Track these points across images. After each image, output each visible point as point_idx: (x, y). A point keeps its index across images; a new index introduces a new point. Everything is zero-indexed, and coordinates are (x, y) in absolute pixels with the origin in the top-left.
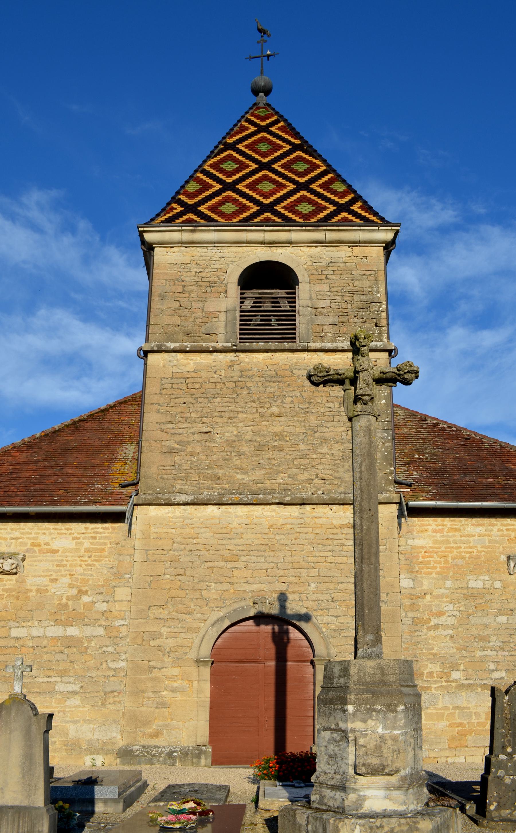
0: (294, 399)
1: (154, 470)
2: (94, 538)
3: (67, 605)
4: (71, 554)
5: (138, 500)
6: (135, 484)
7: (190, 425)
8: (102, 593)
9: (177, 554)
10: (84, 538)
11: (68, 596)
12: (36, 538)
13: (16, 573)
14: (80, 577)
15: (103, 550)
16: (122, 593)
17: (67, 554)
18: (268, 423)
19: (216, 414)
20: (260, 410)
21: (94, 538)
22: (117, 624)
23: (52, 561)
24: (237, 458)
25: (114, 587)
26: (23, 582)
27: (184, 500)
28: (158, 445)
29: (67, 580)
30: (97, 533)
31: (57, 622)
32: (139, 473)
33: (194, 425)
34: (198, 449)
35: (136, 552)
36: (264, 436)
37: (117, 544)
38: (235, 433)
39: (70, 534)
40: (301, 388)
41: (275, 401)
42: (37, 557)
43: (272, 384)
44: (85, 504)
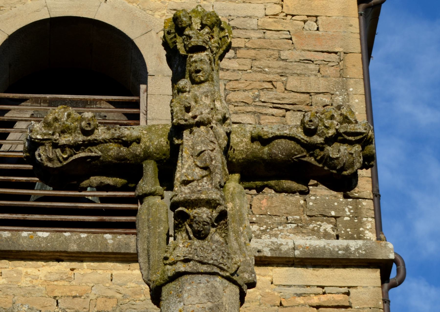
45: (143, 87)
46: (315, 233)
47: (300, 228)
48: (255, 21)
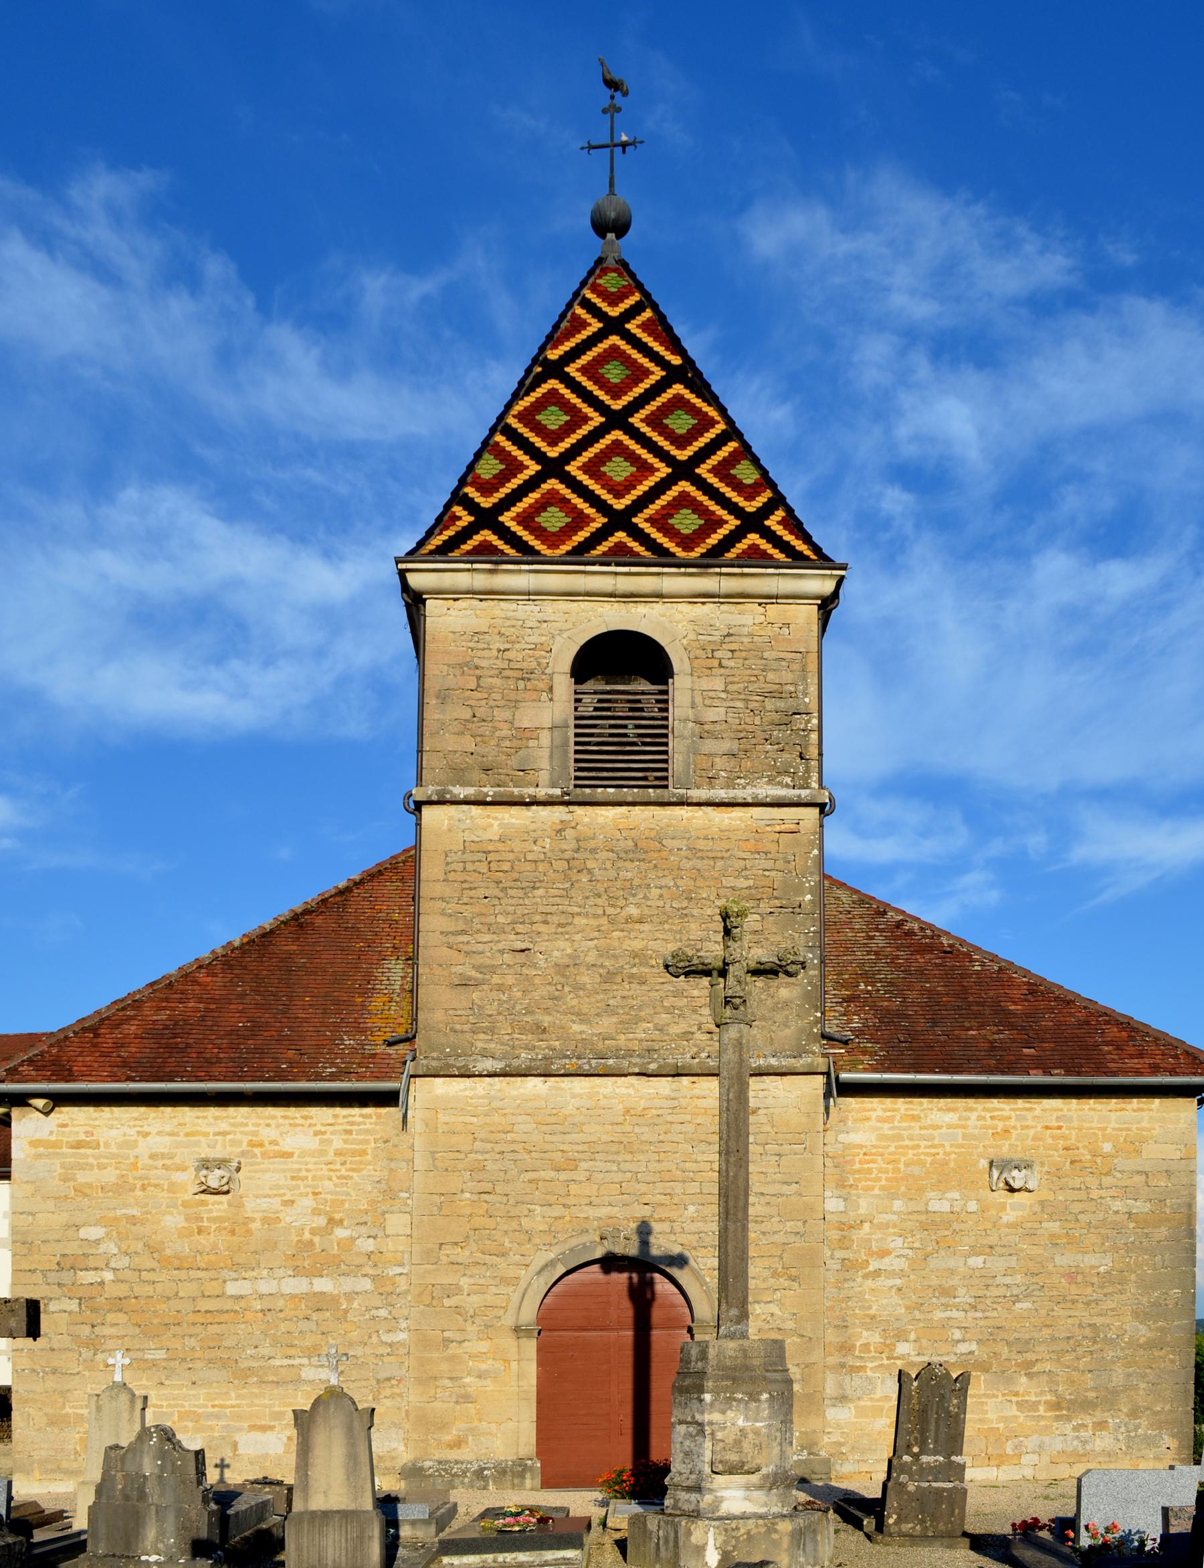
0: (664, 891)
1: (439, 1016)
2: (349, 1132)
3: (311, 1243)
4: (314, 1160)
5: (415, 1068)
6: (410, 1039)
7: (495, 937)
8: (366, 1223)
9: (481, 1158)
10: (333, 1133)
11: (311, 1229)
12: (255, 1133)
13: (228, 1192)
14: (329, 1197)
15: (363, 1153)
16: (397, 1223)
17: (308, 1159)
18: (621, 934)
19: (538, 918)
20: (610, 911)
21: (349, 1132)
22: (391, 1274)
23: (284, 1171)
24: (572, 995)
25: (384, 1213)
26: (240, 1205)
27: (490, 1069)
28: (445, 973)
29: (309, 1202)
30: (352, 1124)
31: (298, 1271)
32: (416, 1020)
33: (503, 936)
34: (510, 980)
35: (417, 1155)
36: (615, 957)
37: (385, 1142)
38: (569, 951)
39: (310, 1125)
40: (676, 872)
41: (634, 895)
42: (259, 1164)
43: (628, 865)
44: (333, 1077)
45: (670, 681)
46: (780, 783)
47: (771, 781)
48: (746, 629)
